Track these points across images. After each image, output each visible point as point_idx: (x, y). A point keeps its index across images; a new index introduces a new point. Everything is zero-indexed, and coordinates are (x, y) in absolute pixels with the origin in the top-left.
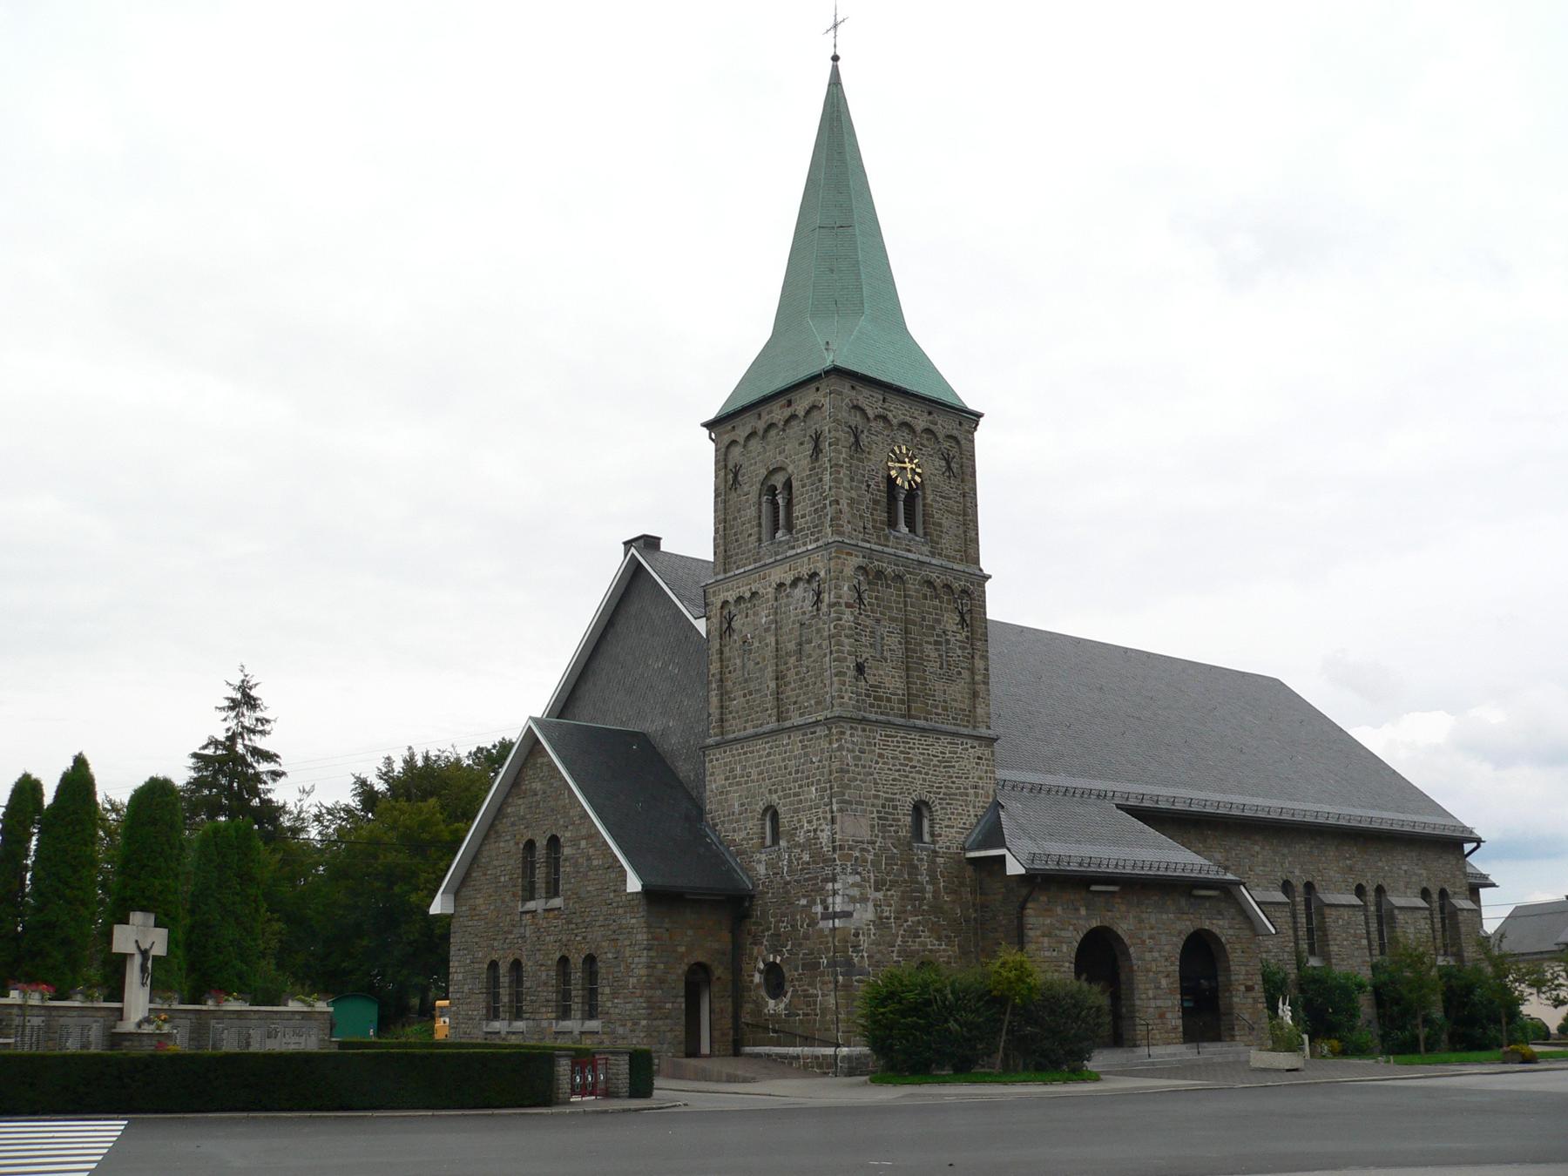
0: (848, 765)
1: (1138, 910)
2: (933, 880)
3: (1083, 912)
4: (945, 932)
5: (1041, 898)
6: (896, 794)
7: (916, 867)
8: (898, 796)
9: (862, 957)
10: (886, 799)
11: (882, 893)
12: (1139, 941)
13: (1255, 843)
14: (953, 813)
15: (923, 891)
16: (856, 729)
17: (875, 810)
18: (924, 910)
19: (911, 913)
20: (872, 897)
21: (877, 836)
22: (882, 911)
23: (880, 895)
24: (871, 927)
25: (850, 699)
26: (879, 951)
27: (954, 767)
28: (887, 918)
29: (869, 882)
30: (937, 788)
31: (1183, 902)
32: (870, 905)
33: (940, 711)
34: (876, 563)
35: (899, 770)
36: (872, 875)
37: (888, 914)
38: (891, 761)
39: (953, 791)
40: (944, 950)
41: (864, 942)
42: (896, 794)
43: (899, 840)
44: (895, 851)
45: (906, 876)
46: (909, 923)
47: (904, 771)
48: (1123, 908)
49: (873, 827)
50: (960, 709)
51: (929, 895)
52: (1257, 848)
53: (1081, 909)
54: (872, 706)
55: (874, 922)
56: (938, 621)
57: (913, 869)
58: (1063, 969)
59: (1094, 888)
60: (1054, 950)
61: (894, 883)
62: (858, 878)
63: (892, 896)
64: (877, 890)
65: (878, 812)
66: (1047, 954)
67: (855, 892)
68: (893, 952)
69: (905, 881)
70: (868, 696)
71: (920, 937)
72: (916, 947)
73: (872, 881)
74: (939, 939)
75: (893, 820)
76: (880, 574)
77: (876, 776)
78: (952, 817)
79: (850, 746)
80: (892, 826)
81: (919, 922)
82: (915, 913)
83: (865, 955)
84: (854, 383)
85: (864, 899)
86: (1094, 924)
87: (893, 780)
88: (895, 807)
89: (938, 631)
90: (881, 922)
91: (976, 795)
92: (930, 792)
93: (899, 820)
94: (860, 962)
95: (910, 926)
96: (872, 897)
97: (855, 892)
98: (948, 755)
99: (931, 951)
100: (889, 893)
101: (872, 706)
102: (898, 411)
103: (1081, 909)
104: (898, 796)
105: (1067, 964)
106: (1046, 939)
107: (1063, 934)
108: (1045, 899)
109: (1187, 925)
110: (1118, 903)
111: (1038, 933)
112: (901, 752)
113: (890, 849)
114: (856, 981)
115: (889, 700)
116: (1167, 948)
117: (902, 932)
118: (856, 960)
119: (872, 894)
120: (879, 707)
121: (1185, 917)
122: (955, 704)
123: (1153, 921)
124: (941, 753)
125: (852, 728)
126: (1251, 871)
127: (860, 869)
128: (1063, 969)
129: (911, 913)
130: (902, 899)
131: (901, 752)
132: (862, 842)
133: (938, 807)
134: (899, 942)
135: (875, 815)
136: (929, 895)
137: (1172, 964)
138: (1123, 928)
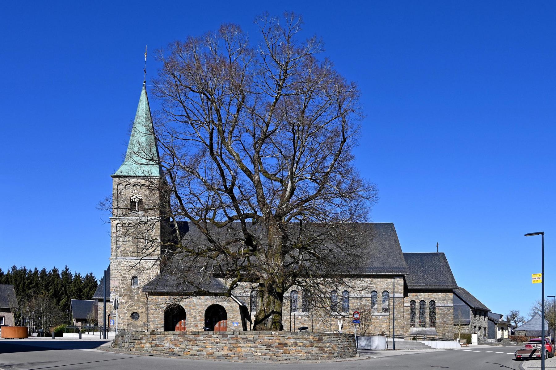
0: (112, 269)
2: (138, 294)
4: (141, 306)
7: (133, 291)
10: (124, 276)
15: (134, 296)
16: (115, 261)
17: (120, 279)
18: (134, 301)
19: (130, 301)
23: (121, 298)
25: (114, 254)
27: (146, 267)
28: (123, 303)
34: (123, 221)
36: (119, 293)
37: (123, 302)
38: (126, 267)
39: (145, 273)
40: (140, 310)
43: (127, 285)
44: (126, 288)
45: (129, 293)
49: (119, 283)
51: (136, 298)
54: (122, 255)
57: (131, 292)
61: (125, 295)
62: (115, 294)
63: (125, 298)
64: (120, 296)
65: (121, 279)
69: (129, 294)
70: (121, 253)
73: (119, 295)
74: (139, 307)
75: (126, 281)
79: (113, 265)
80: (125, 282)
82: (132, 301)
88: (126, 278)
91: (153, 273)
93: (128, 281)
99: (136, 310)
104: (127, 275)
115: (127, 253)
118: (113, 312)
120: (124, 255)
123: (195, 302)
125: (114, 261)
127: (115, 292)
129: (130, 301)
130: (128, 298)
132: (117, 286)
134: (126, 308)
135: (120, 280)
136: (136, 298)
138: (183, 304)
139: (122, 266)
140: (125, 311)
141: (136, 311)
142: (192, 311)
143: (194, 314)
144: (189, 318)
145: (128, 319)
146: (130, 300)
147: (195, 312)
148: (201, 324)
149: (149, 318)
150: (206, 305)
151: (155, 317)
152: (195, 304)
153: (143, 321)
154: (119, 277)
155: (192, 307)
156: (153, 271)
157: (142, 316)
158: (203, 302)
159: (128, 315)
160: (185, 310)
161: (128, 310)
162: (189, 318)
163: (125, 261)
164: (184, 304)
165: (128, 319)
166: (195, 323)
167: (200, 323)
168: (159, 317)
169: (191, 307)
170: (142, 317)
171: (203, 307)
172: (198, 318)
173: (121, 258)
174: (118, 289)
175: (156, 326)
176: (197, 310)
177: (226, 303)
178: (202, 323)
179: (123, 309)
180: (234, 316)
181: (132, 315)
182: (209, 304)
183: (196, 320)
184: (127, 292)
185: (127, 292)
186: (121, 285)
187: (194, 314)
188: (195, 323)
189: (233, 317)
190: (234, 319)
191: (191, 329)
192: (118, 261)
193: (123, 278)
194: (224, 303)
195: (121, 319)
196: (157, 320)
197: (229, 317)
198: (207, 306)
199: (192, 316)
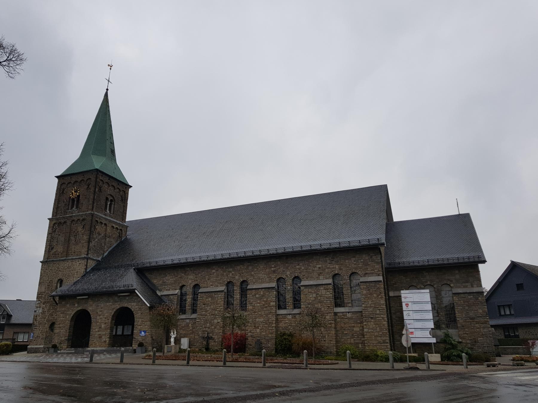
1: (97, 303)
3: (76, 305)
5: (63, 303)
6: (53, 278)
8: (54, 279)
9: (37, 322)
10: (50, 280)
11: (45, 305)
12: (95, 313)
13: (214, 269)
14: (69, 281)
16: (45, 264)
20: (42, 306)
21: (46, 290)
22: (44, 310)
23: (44, 306)
24: (41, 314)
26: (41, 320)
28: (45, 311)
29: (42, 302)
30: (65, 275)
31: (116, 298)
32: (41, 308)
33: (73, 253)
35: (55, 272)
39: (70, 275)
42: (53, 278)
46: (51, 312)
47: (57, 272)
48: (91, 303)
50: (79, 251)
52: (214, 271)
53: (76, 304)
54: (54, 257)
55: (41, 313)
56: (76, 230)
58: (65, 323)
59: (78, 298)
60: (64, 318)
62: (39, 302)
63: (47, 305)
64: (44, 304)
66: (61, 319)
68: (45, 320)
70: (53, 255)
71: (53, 316)
73: (43, 302)
75: (51, 285)
76: (60, 223)
77: (49, 275)
78: (68, 282)
81: (53, 312)
83: (38, 321)
84: (63, 178)
85: (40, 307)
86: (79, 309)
87: (53, 275)
88: (52, 282)
89: (76, 232)
90: (43, 313)
91: (77, 274)
92: (63, 276)
94: (36, 323)
95: (51, 313)
96: (42, 306)
98: (70, 265)
100: (47, 305)
101: (54, 257)
103: (76, 304)
105: (67, 322)
106: (62, 315)
107: (68, 312)
108: (64, 303)
109: (117, 306)
110: (89, 301)
111: (60, 313)
112: (57, 267)
113: (49, 293)
114: (35, 328)
115: (58, 254)
116: (106, 314)
117: (48, 315)
121: (116, 303)
122: (77, 251)
124: (68, 265)
125: (44, 264)
126: (209, 280)
128: (65, 323)
130: (50, 306)
131: (57, 267)
133: (65, 280)
137: (108, 320)
138: (90, 309)
139: (51, 269)
140: (45, 321)
143: (100, 321)
146: (51, 308)
147: (101, 319)
148: (106, 334)
149: (55, 329)
150: (114, 309)
151: (60, 327)
152: (102, 308)
154: (46, 282)
155: (99, 313)
156: (77, 272)
158: (111, 305)
160: (92, 316)
161: (48, 321)
164: (91, 309)
165: (47, 331)
166: (99, 333)
167: (104, 333)
168: (64, 327)
169: (98, 313)
171: (110, 311)
172: (103, 326)
174: (43, 296)
175: (61, 338)
176: (104, 316)
177: (135, 304)
178: (107, 333)
180: (142, 321)
182: (117, 306)
183: (101, 329)
186: (46, 291)
188: (99, 333)
189: (141, 323)
190: (141, 327)
191: (94, 341)
192: (47, 264)
193: (49, 282)
194: (133, 304)
195: (40, 331)
196: (62, 331)
197: (137, 323)
198: (115, 310)
199: (98, 323)
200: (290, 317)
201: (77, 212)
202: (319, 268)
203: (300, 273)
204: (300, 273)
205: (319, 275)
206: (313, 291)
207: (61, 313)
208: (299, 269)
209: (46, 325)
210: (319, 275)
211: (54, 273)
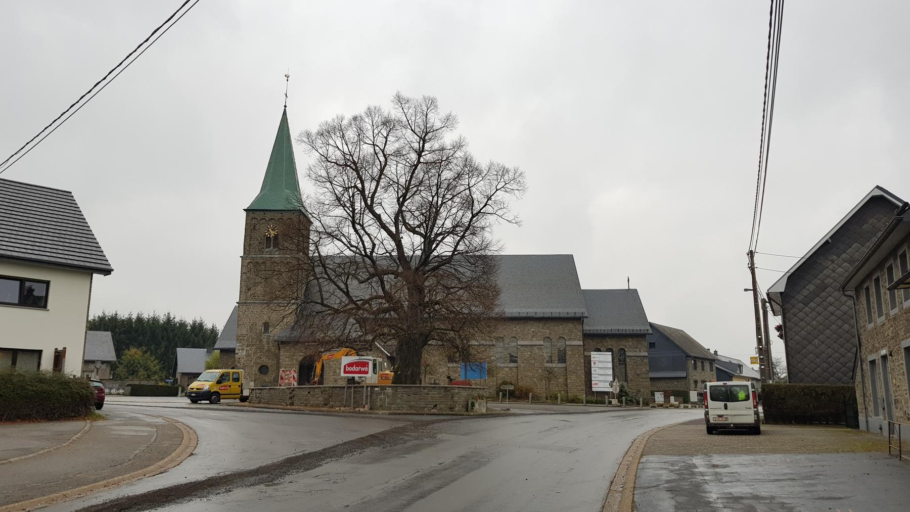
2: (268, 343)
5: (287, 348)
23: (249, 348)
41: (242, 361)
43: (257, 333)
49: (247, 331)
54: (252, 298)
57: (261, 341)
62: (241, 344)
67: (240, 348)
70: (251, 296)
72: (260, 361)
74: (269, 359)
82: (261, 352)
90: (248, 355)
97: (240, 348)
101: (252, 298)
102: (268, 216)
115: (258, 296)
119: (245, 348)
136: (266, 348)
139: (252, 312)
141: (265, 364)
142: (331, 363)
144: (328, 372)
145: (255, 374)
147: (335, 364)
153: (273, 376)
157: (272, 370)
159: (255, 369)
161: (256, 363)
162: (328, 372)
163: (255, 305)
165: (255, 374)
170: (272, 371)
173: (251, 302)
179: (250, 361)
181: (260, 368)
184: (256, 342)
185: (256, 342)
187: (334, 366)
200: (507, 369)
201: (277, 253)
202: (533, 331)
203: (516, 334)
204: (516, 334)
205: (532, 337)
206: (528, 350)
207: (286, 358)
208: (516, 331)
209: (254, 368)
210: (532, 337)
211: (257, 316)
